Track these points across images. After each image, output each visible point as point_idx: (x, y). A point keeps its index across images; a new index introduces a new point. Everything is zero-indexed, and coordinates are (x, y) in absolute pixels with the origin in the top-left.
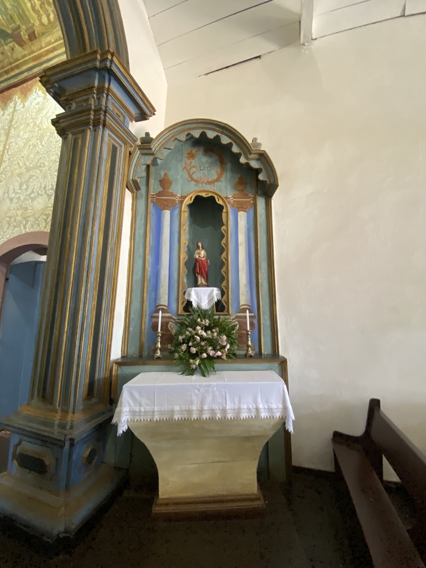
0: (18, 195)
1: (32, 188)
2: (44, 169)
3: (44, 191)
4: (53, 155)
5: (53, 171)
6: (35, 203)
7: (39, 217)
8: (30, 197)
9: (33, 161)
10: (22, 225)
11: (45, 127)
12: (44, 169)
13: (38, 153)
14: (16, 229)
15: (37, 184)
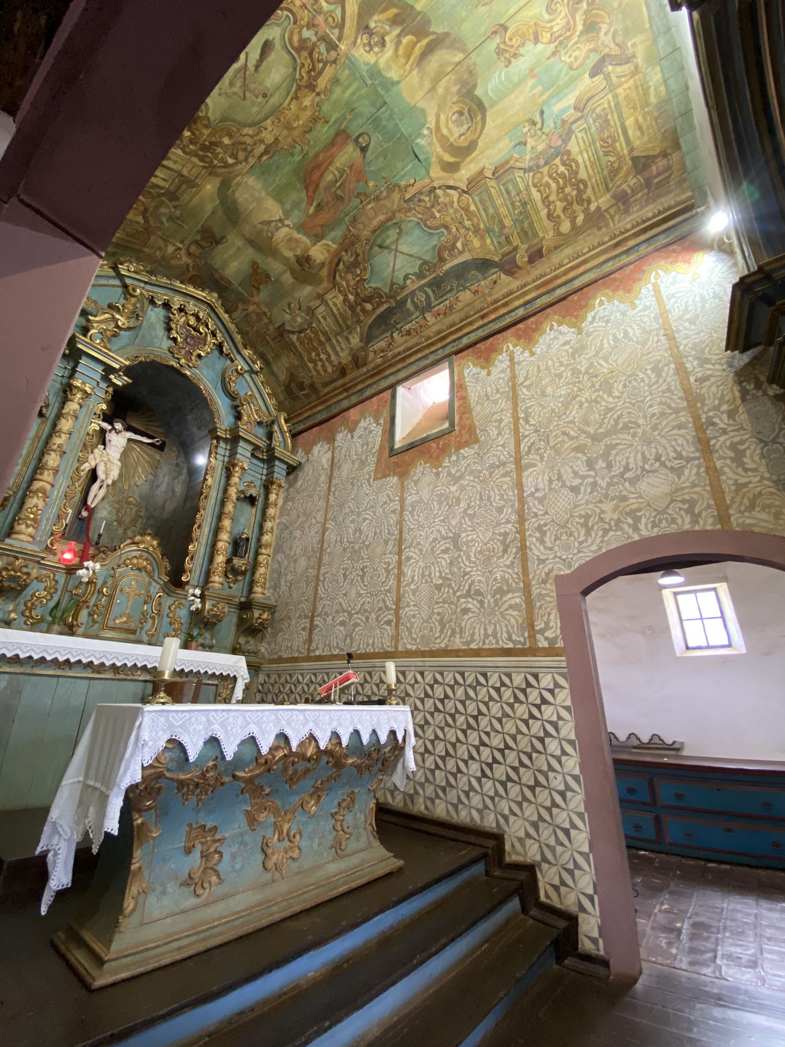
0: (591, 480)
1: (624, 463)
2: (640, 431)
3: (657, 464)
4: (651, 406)
5: (666, 430)
6: (643, 486)
7: (667, 507)
8: (625, 480)
9: (602, 423)
10: (626, 527)
11: (606, 371)
12: (640, 431)
13: (608, 410)
14: (611, 533)
15: (632, 455)
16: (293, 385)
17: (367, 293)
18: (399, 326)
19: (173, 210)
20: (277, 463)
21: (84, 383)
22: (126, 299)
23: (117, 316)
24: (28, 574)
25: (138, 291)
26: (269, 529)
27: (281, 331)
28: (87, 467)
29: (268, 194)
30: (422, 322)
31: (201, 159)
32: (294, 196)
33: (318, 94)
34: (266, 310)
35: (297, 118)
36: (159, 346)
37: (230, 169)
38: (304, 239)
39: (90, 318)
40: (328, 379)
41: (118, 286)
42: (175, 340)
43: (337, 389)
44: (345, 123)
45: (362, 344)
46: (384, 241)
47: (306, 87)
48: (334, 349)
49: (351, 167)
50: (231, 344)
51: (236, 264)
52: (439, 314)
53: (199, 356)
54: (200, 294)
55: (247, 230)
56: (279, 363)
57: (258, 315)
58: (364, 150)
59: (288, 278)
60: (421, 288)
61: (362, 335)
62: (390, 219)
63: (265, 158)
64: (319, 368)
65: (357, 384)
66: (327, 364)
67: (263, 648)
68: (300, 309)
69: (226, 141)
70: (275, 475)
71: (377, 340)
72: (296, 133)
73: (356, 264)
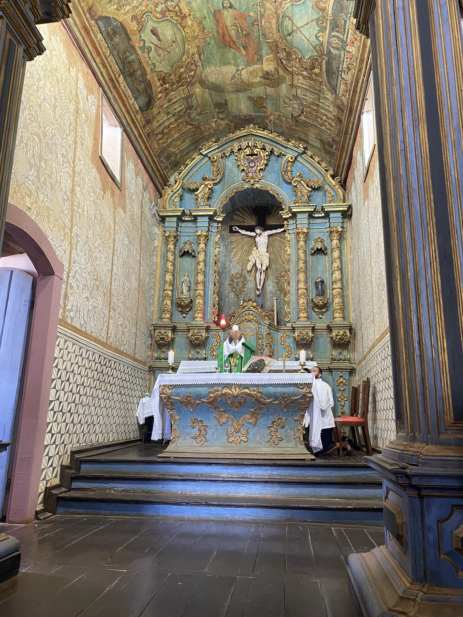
16: (326, 146)
17: (309, 64)
18: (340, 69)
19: (196, 111)
20: (332, 215)
21: (202, 231)
22: (213, 165)
23: (207, 183)
24: (201, 335)
25: (215, 157)
26: (336, 269)
27: (295, 119)
28: (250, 264)
29: (220, 67)
30: (349, 55)
31: (182, 85)
32: (230, 55)
33: (189, 15)
34: (278, 113)
35: (194, 31)
36: (237, 180)
37: (196, 76)
38: (255, 66)
39: (196, 193)
40: (338, 131)
41: (207, 161)
42: (243, 170)
43: (341, 136)
44: (212, 9)
45: (334, 95)
46: (288, 31)
47: (182, 20)
48: (325, 110)
49: (235, 19)
50: (278, 146)
51: (243, 105)
52: (353, 42)
53: (261, 169)
54: (243, 132)
55: (230, 88)
56: (310, 138)
57: (277, 119)
58: (231, 7)
59: (269, 90)
60: (330, 37)
61: (329, 90)
62: (278, 18)
63: (202, 57)
64: (328, 126)
65: (348, 127)
66: (330, 121)
67: (356, 356)
68: (291, 100)
69: (182, 70)
70: (331, 226)
71: (338, 87)
72: (200, 36)
73: (289, 54)
